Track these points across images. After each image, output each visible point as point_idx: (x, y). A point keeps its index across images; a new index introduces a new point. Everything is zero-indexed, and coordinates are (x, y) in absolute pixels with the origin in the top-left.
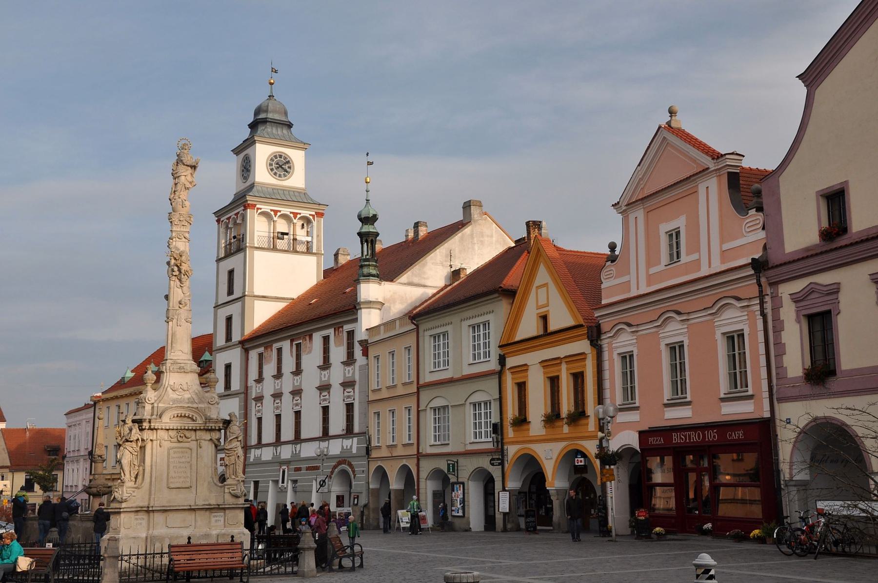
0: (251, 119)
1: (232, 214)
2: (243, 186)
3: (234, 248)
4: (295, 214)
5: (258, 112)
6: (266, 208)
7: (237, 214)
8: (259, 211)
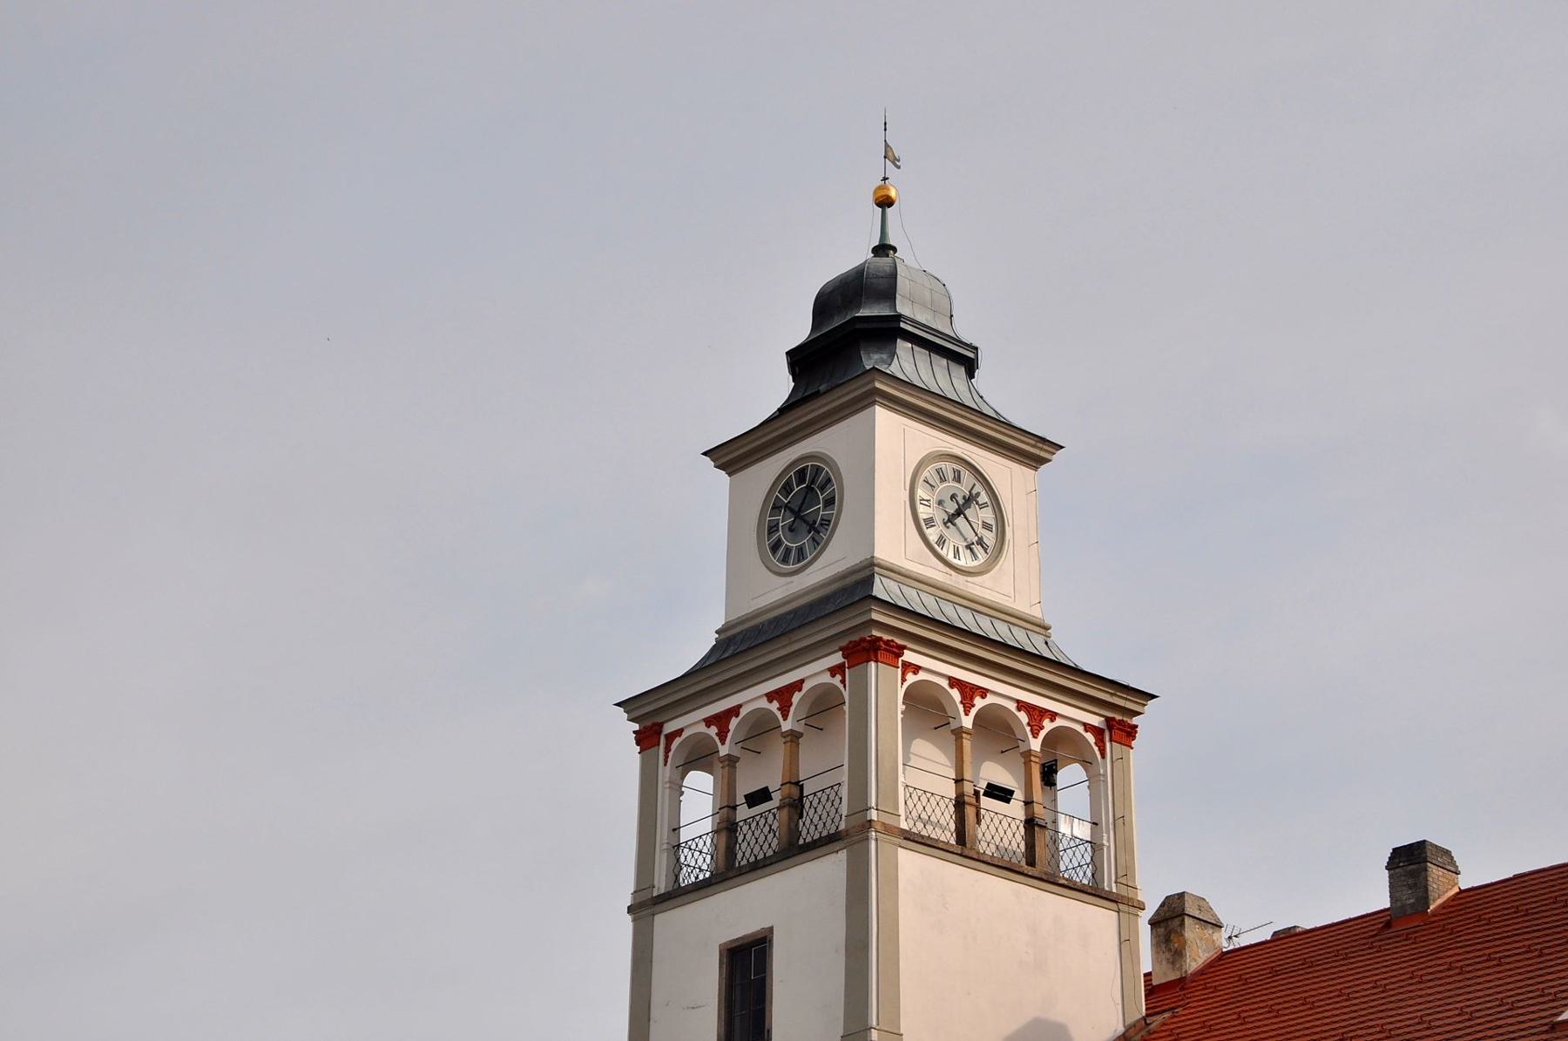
0: (800, 330)
1: (753, 698)
2: (775, 590)
3: (755, 841)
4: (1037, 715)
5: (824, 305)
6: (936, 669)
7: (783, 696)
8: (911, 678)
